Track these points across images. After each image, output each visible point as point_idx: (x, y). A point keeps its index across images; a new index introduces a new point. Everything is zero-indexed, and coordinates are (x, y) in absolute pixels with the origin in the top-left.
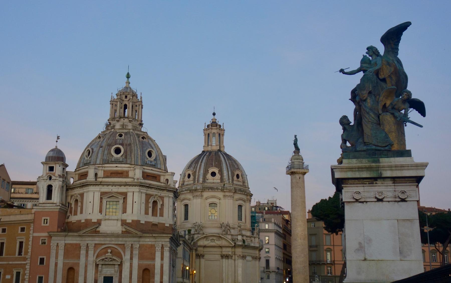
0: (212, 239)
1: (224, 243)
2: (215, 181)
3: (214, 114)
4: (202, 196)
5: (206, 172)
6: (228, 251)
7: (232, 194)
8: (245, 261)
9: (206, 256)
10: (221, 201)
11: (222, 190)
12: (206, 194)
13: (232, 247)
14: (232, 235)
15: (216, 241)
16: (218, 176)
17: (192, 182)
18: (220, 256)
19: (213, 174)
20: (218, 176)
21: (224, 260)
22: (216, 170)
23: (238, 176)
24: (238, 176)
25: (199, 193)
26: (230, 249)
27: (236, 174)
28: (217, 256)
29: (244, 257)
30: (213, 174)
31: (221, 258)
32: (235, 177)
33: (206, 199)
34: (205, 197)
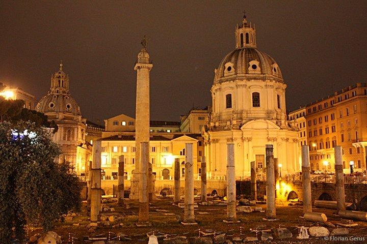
2: (256, 72)
12: (249, 83)
16: (258, 68)
19: (254, 67)
20: (258, 68)
22: (256, 63)
29: (287, 140)
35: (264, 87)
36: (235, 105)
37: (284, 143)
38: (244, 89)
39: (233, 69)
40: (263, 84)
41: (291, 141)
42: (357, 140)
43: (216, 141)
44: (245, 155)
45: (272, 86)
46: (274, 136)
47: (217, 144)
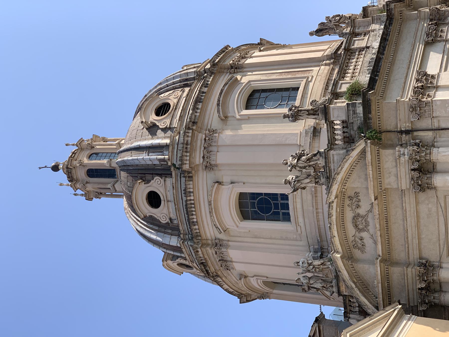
0: (356, 226)
3: (55, 168)
4: (218, 244)
6: (396, 166)
9: (431, 253)
10: (226, 179)
11: (188, 175)
15: (362, 211)
16: (156, 185)
18: (422, 196)
19: (154, 200)
21: (438, 180)
23: (163, 109)
24: (163, 109)
27: (153, 118)
28: (423, 208)
31: (431, 193)
32: (163, 121)
38: (233, 254)
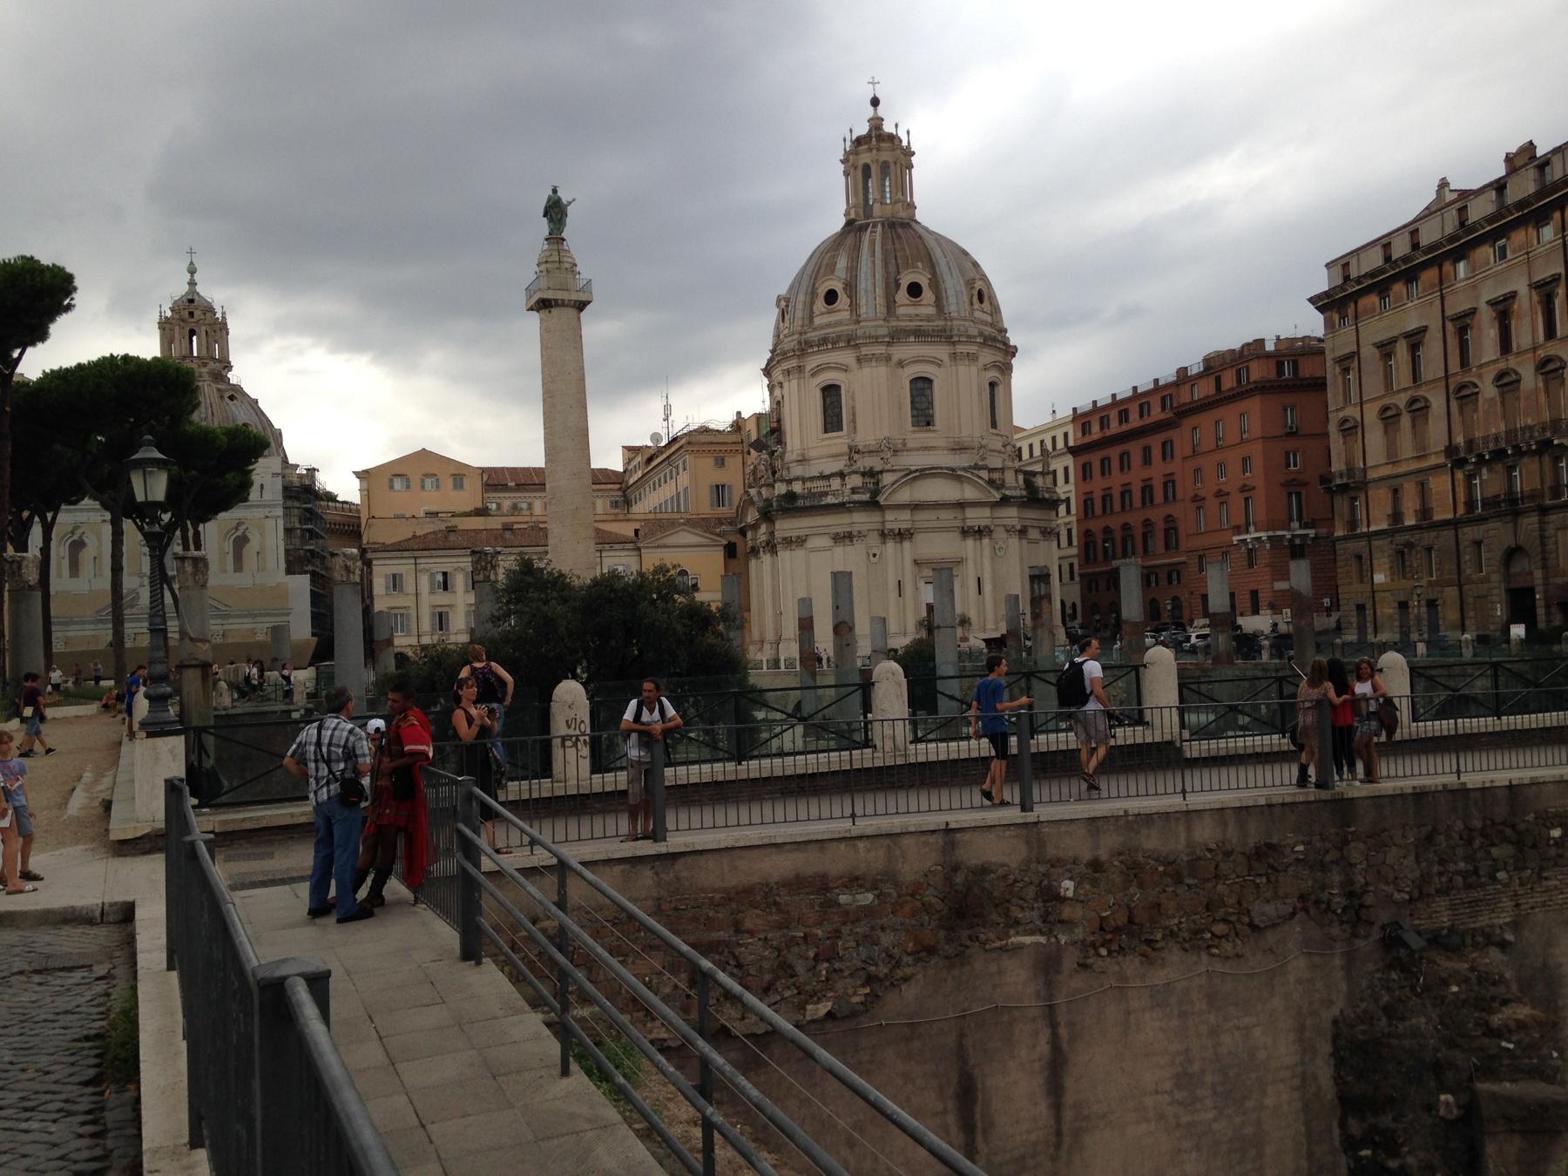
1: (970, 493)
3: (875, 102)
4: (888, 358)
5: (892, 285)
7: (973, 349)
8: (1024, 542)
12: (899, 352)
13: (994, 505)
14: (991, 470)
17: (846, 315)
19: (915, 290)
20: (928, 295)
25: (880, 350)
26: (987, 512)
29: (1023, 532)
30: (915, 290)
33: (901, 364)
34: (895, 358)
35: (946, 358)
36: (854, 421)
37: (1014, 542)
38: (882, 370)
39: (843, 300)
40: (942, 351)
41: (1034, 534)
42: (1248, 525)
43: (800, 541)
44: (892, 585)
45: (972, 358)
46: (983, 523)
47: (800, 553)
